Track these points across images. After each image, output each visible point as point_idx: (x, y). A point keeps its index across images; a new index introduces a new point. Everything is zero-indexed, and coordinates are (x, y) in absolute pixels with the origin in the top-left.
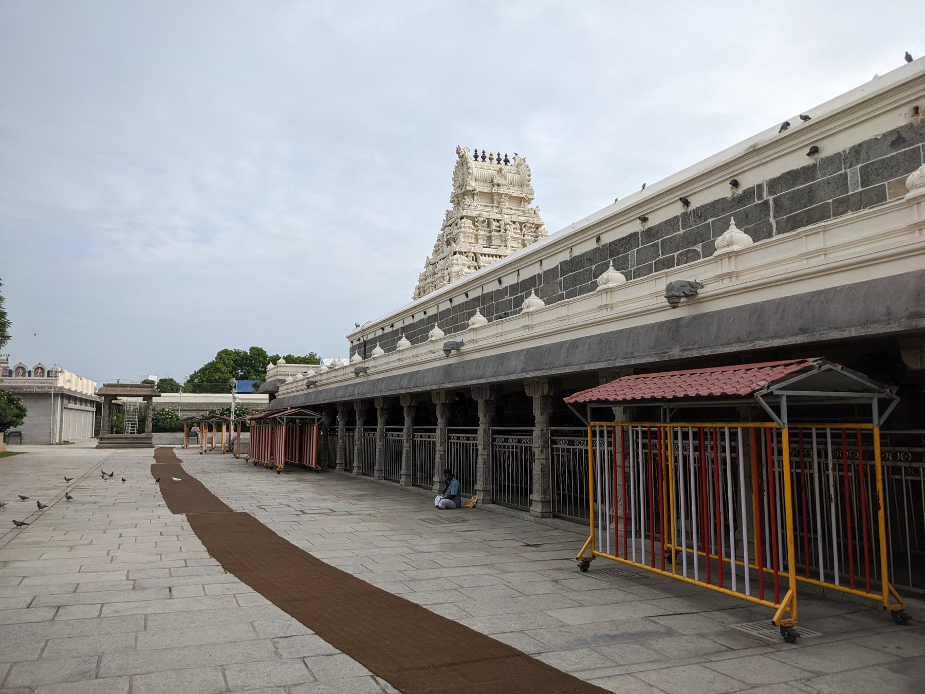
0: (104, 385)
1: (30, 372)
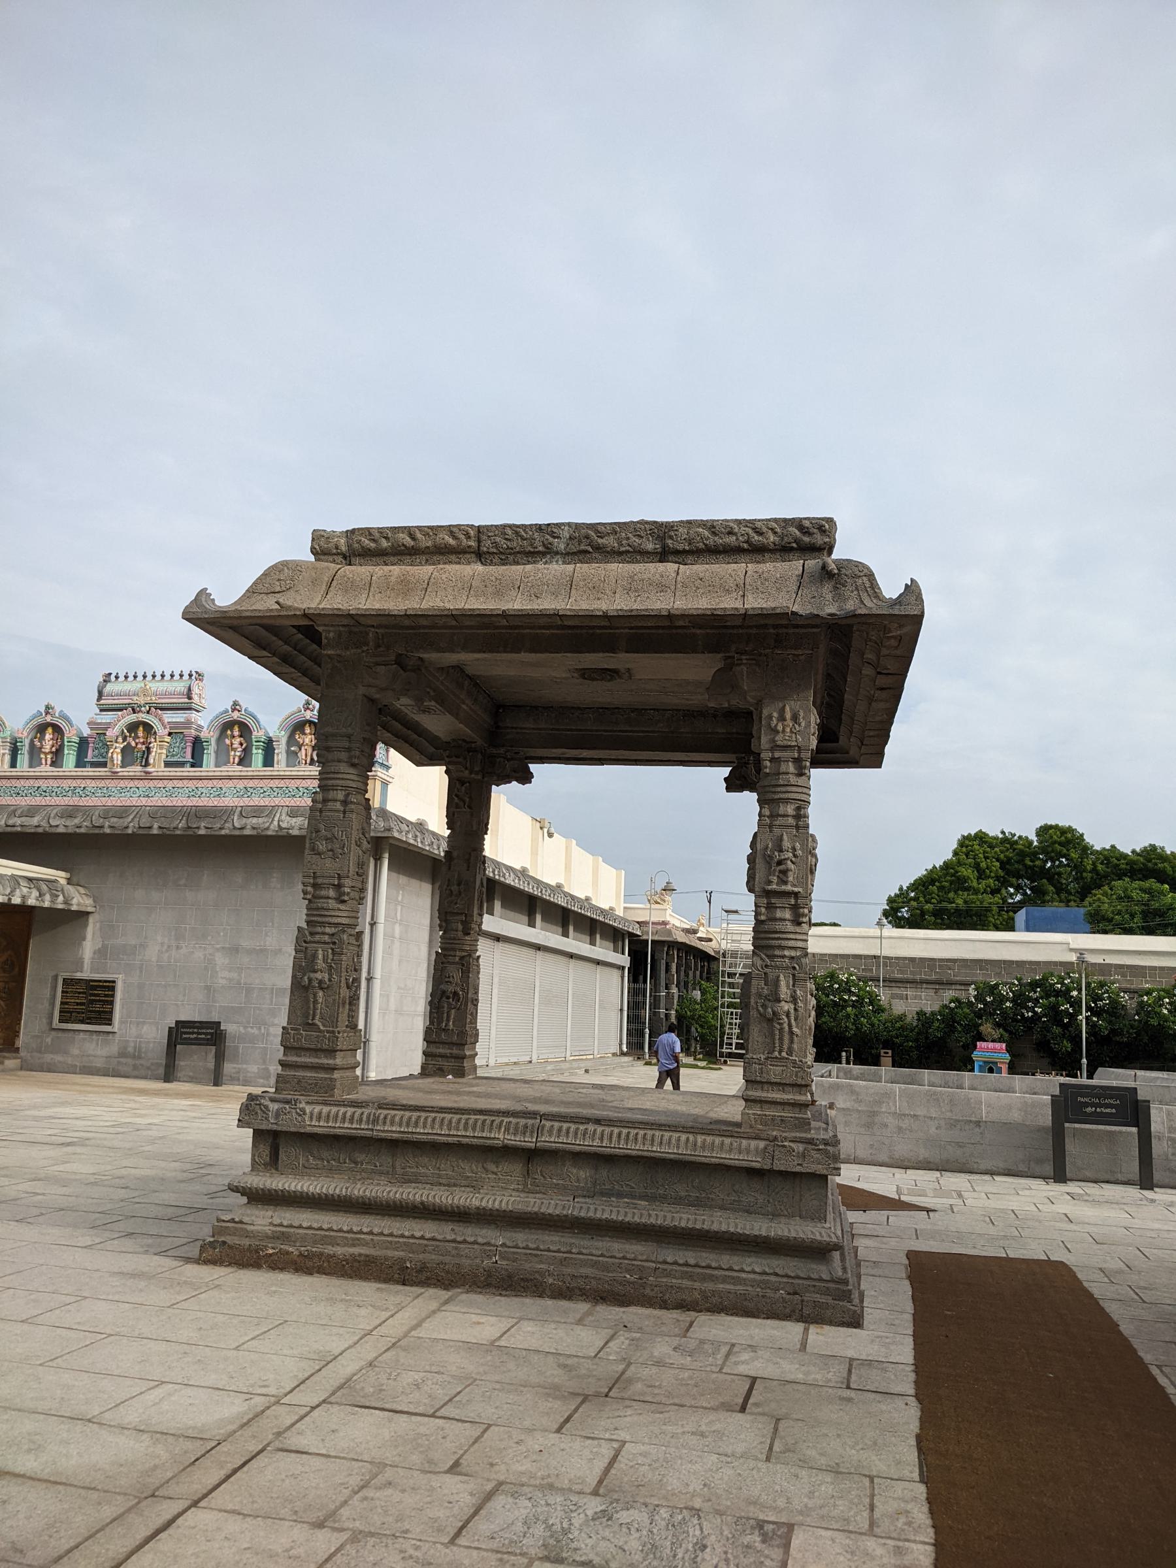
0: (323, 546)
1: (269, 748)
